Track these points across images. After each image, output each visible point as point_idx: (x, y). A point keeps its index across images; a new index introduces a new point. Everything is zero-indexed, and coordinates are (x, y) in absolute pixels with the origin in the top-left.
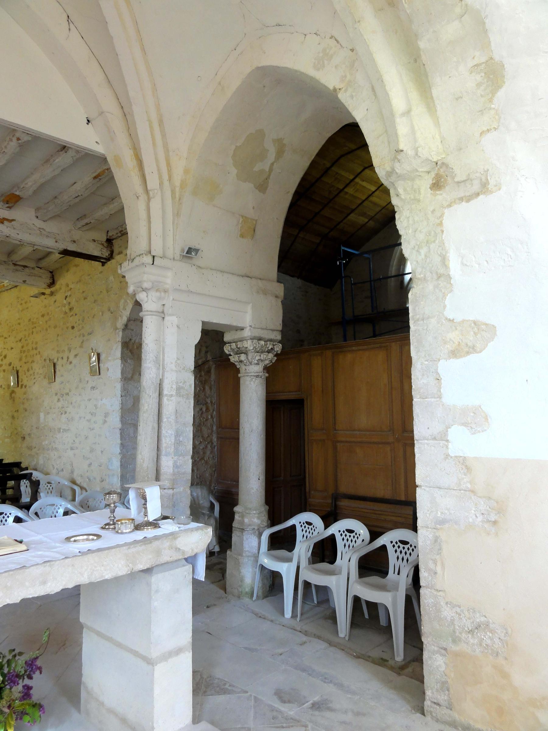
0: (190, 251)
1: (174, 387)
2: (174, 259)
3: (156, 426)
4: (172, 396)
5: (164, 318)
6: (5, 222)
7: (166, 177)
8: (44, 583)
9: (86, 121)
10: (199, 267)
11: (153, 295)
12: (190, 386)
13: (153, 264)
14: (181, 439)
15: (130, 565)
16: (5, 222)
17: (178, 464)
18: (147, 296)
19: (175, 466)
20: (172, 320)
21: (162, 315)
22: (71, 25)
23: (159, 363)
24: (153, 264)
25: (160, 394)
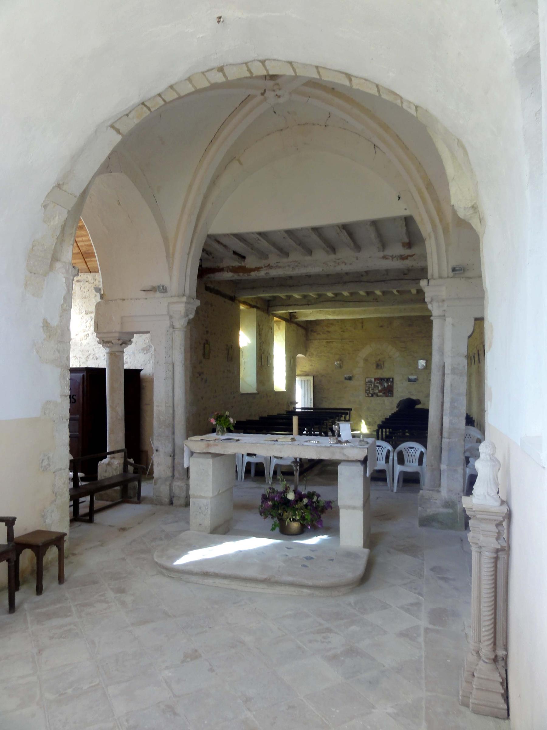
0: (454, 270)
1: (450, 368)
2: (448, 277)
3: (440, 395)
4: (448, 374)
5: (445, 320)
6: (409, 258)
7: (437, 221)
8: (281, 452)
9: (398, 198)
10: (469, 278)
11: (435, 304)
12: (464, 367)
13: (428, 285)
14: (456, 404)
15: (318, 455)
16: (409, 258)
17: (453, 422)
18: (432, 306)
19: (451, 422)
20: (449, 320)
21: (443, 317)
22: (377, 149)
23: (442, 352)
24: (428, 285)
25: (444, 374)
